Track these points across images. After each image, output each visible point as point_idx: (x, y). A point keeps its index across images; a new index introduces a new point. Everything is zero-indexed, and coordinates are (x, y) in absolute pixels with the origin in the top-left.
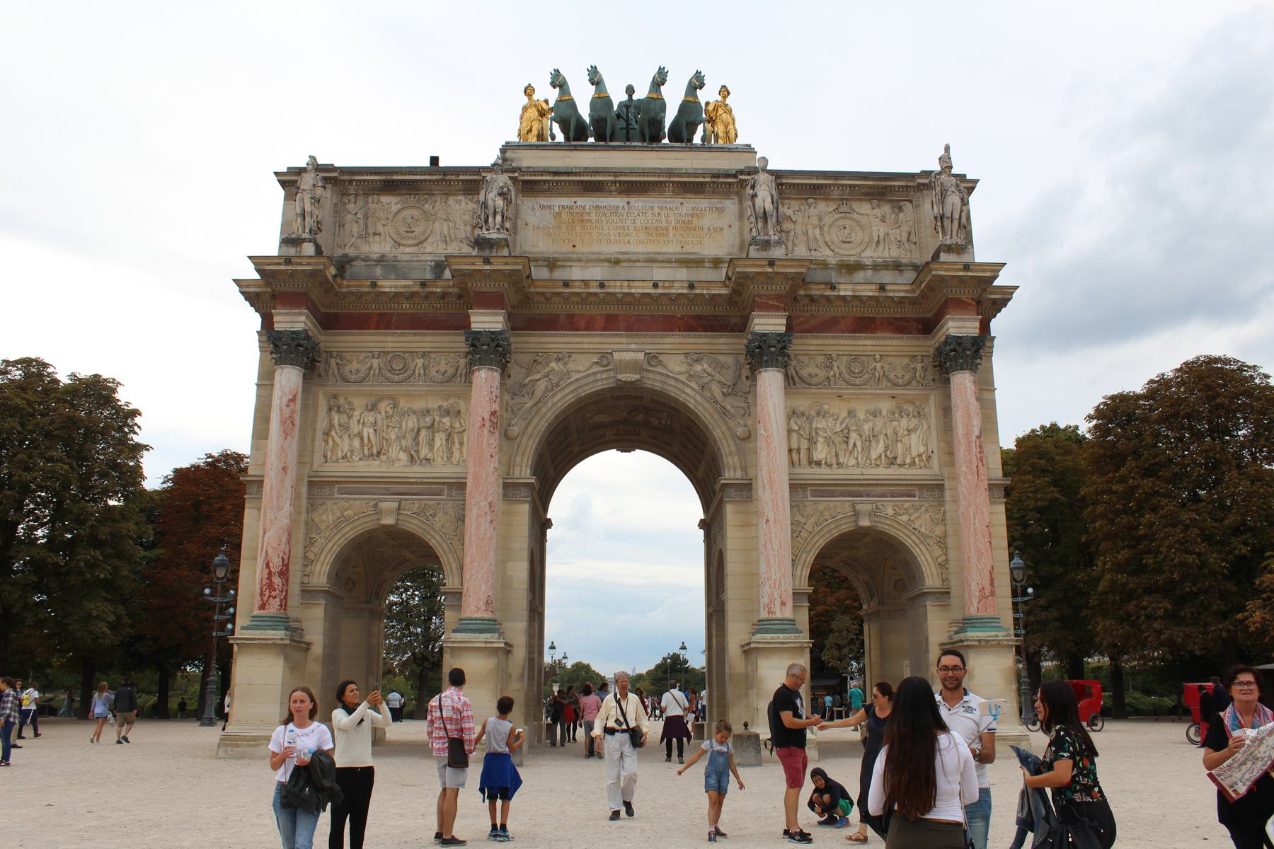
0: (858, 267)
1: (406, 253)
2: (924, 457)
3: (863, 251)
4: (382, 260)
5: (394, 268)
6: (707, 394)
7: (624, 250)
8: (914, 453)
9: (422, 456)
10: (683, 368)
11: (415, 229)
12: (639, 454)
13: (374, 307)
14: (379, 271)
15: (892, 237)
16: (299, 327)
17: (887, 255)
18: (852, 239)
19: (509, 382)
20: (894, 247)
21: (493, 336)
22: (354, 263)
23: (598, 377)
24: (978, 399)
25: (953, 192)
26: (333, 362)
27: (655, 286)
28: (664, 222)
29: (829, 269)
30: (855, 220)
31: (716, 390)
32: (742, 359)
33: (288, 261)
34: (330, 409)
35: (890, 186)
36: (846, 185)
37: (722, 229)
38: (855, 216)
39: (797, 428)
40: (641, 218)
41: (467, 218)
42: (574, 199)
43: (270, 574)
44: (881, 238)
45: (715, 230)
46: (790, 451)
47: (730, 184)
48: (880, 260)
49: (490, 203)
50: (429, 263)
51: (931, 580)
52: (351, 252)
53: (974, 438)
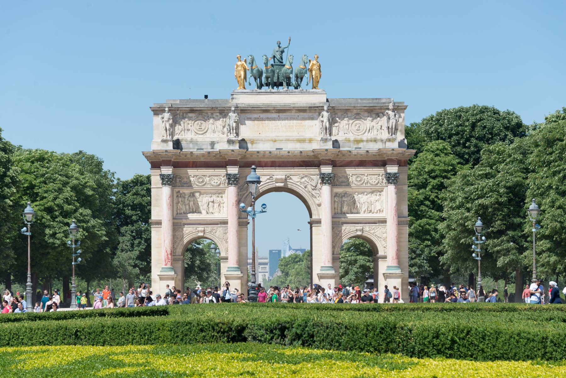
0: (362, 141)
1: (199, 138)
2: (381, 210)
4: (192, 141)
6: (306, 189)
8: (378, 209)
9: (210, 212)
10: (298, 180)
12: (283, 193)
14: (191, 145)
16: (170, 172)
19: (239, 185)
20: (375, 132)
21: (235, 175)
23: (269, 184)
24: (396, 194)
26: (178, 180)
31: (309, 187)
32: (318, 177)
33: (166, 151)
34: (177, 196)
37: (313, 126)
39: (337, 201)
42: (259, 115)
43: (168, 254)
44: (371, 128)
45: (310, 126)
46: (335, 208)
48: (370, 137)
49: (231, 125)
51: (381, 253)
52: (180, 137)
53: (393, 207)
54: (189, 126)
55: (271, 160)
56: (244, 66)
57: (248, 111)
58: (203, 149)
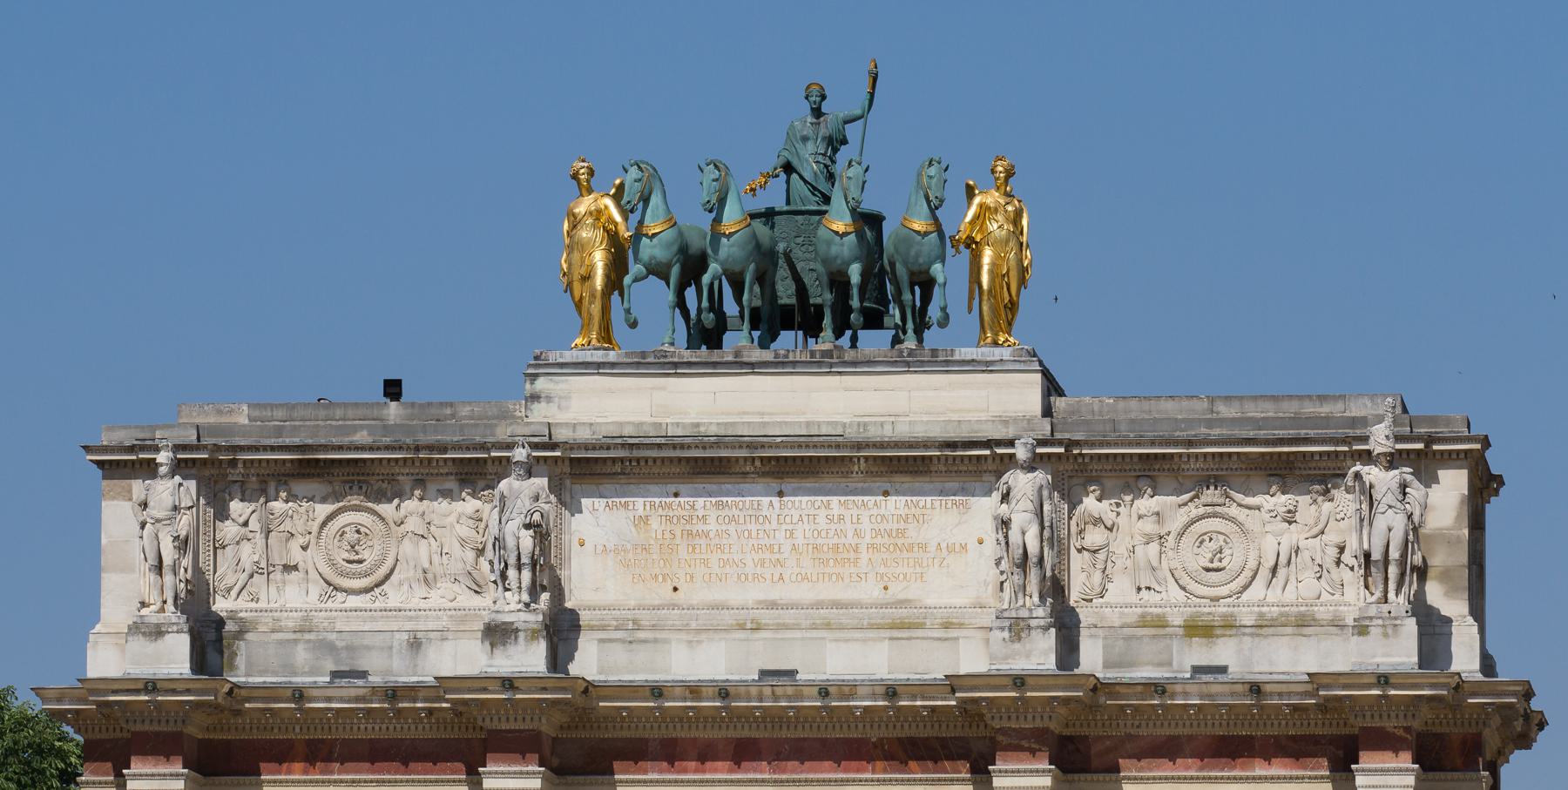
0: (1230, 626)
3: (1246, 587)
5: (330, 648)
7: (775, 594)
11: (365, 555)
13: (297, 730)
14: (301, 655)
15: (1305, 556)
17: (1290, 595)
18: (1224, 563)
20: (1308, 577)
22: (249, 636)
25: (1390, 507)
27: (824, 692)
28: (850, 534)
29: (1171, 636)
30: (1232, 520)
35: (1304, 454)
36: (1213, 454)
37: (964, 547)
38: (1233, 511)
40: (806, 526)
41: (464, 530)
44: (1283, 560)
45: (951, 549)
47: (978, 457)
49: (510, 542)
50: (397, 635)
54: (295, 545)
55: (732, 734)
56: (611, 220)
57: (608, 469)
58: (363, 674)
